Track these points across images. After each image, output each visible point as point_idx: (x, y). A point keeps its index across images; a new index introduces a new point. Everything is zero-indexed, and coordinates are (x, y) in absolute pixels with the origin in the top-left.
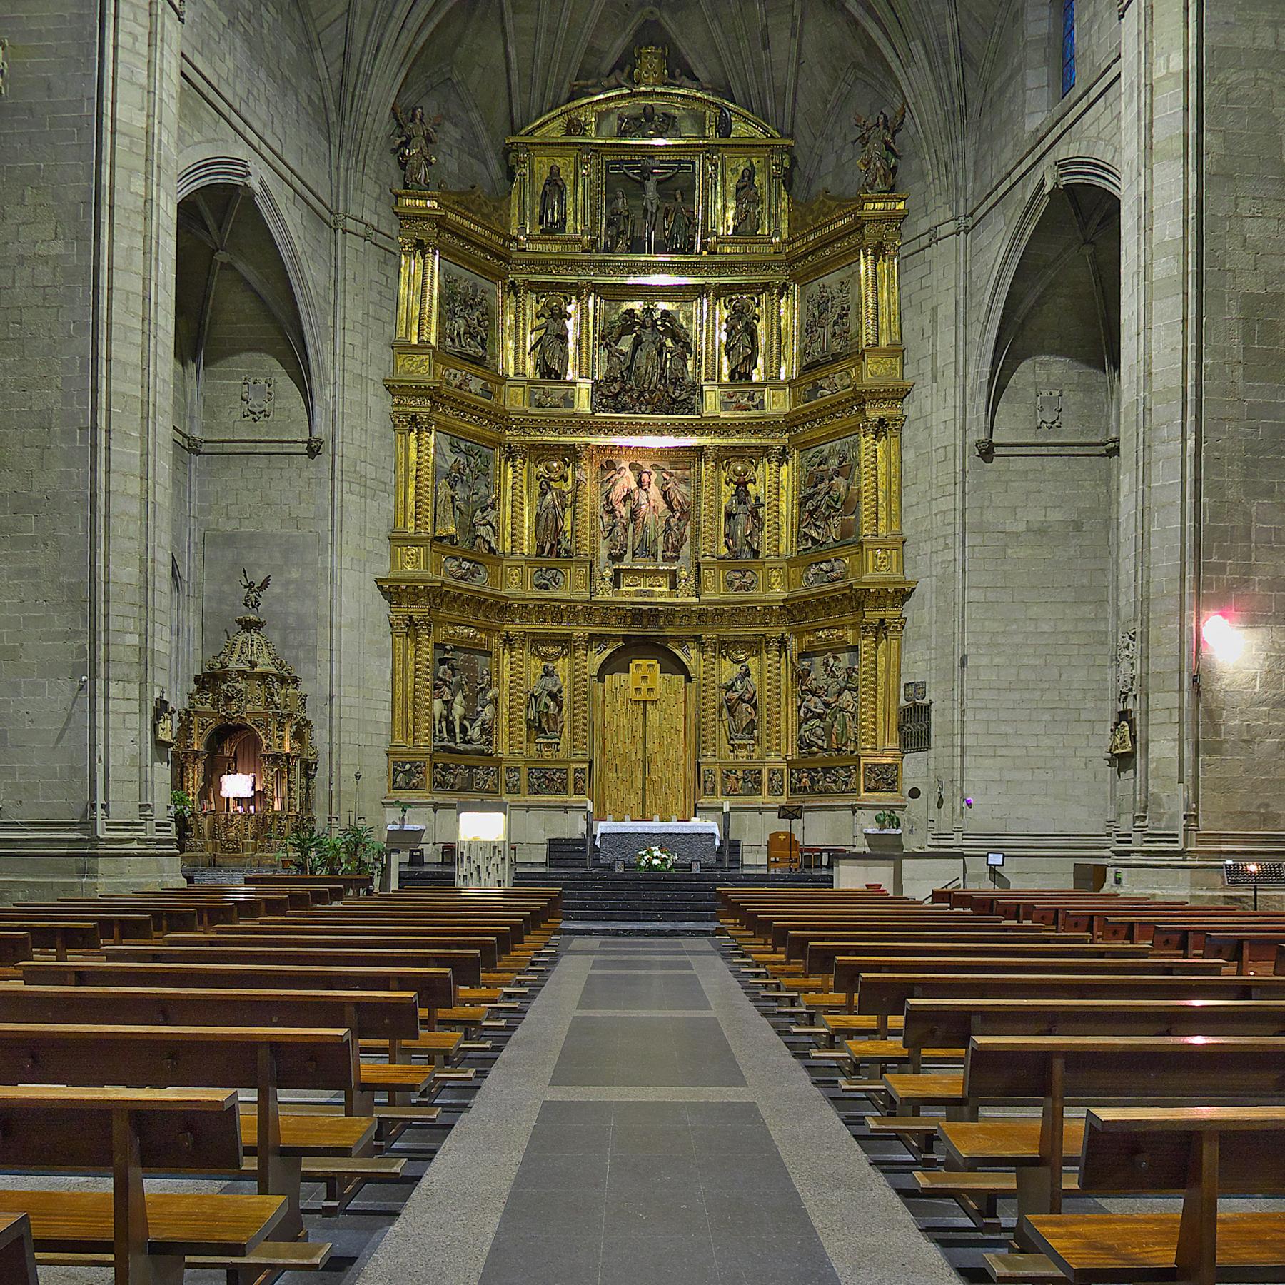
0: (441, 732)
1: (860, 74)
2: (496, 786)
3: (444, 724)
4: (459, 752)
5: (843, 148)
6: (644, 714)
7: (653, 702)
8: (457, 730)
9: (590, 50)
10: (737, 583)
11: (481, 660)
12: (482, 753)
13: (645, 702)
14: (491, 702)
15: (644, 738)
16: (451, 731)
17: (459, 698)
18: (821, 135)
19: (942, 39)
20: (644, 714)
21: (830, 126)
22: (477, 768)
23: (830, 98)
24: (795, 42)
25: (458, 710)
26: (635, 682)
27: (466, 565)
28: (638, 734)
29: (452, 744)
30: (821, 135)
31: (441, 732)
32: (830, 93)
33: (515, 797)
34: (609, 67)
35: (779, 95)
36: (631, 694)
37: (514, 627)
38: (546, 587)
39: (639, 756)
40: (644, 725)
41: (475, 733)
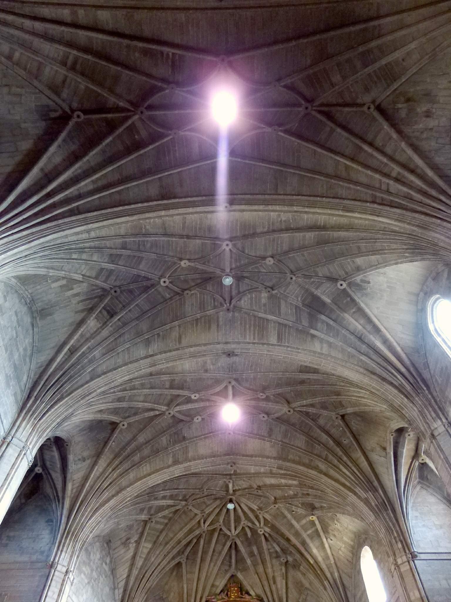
1: (309, 592)
9: (213, 586)
19: (335, 580)
24: (284, 581)
32: (299, 598)
34: (219, 591)
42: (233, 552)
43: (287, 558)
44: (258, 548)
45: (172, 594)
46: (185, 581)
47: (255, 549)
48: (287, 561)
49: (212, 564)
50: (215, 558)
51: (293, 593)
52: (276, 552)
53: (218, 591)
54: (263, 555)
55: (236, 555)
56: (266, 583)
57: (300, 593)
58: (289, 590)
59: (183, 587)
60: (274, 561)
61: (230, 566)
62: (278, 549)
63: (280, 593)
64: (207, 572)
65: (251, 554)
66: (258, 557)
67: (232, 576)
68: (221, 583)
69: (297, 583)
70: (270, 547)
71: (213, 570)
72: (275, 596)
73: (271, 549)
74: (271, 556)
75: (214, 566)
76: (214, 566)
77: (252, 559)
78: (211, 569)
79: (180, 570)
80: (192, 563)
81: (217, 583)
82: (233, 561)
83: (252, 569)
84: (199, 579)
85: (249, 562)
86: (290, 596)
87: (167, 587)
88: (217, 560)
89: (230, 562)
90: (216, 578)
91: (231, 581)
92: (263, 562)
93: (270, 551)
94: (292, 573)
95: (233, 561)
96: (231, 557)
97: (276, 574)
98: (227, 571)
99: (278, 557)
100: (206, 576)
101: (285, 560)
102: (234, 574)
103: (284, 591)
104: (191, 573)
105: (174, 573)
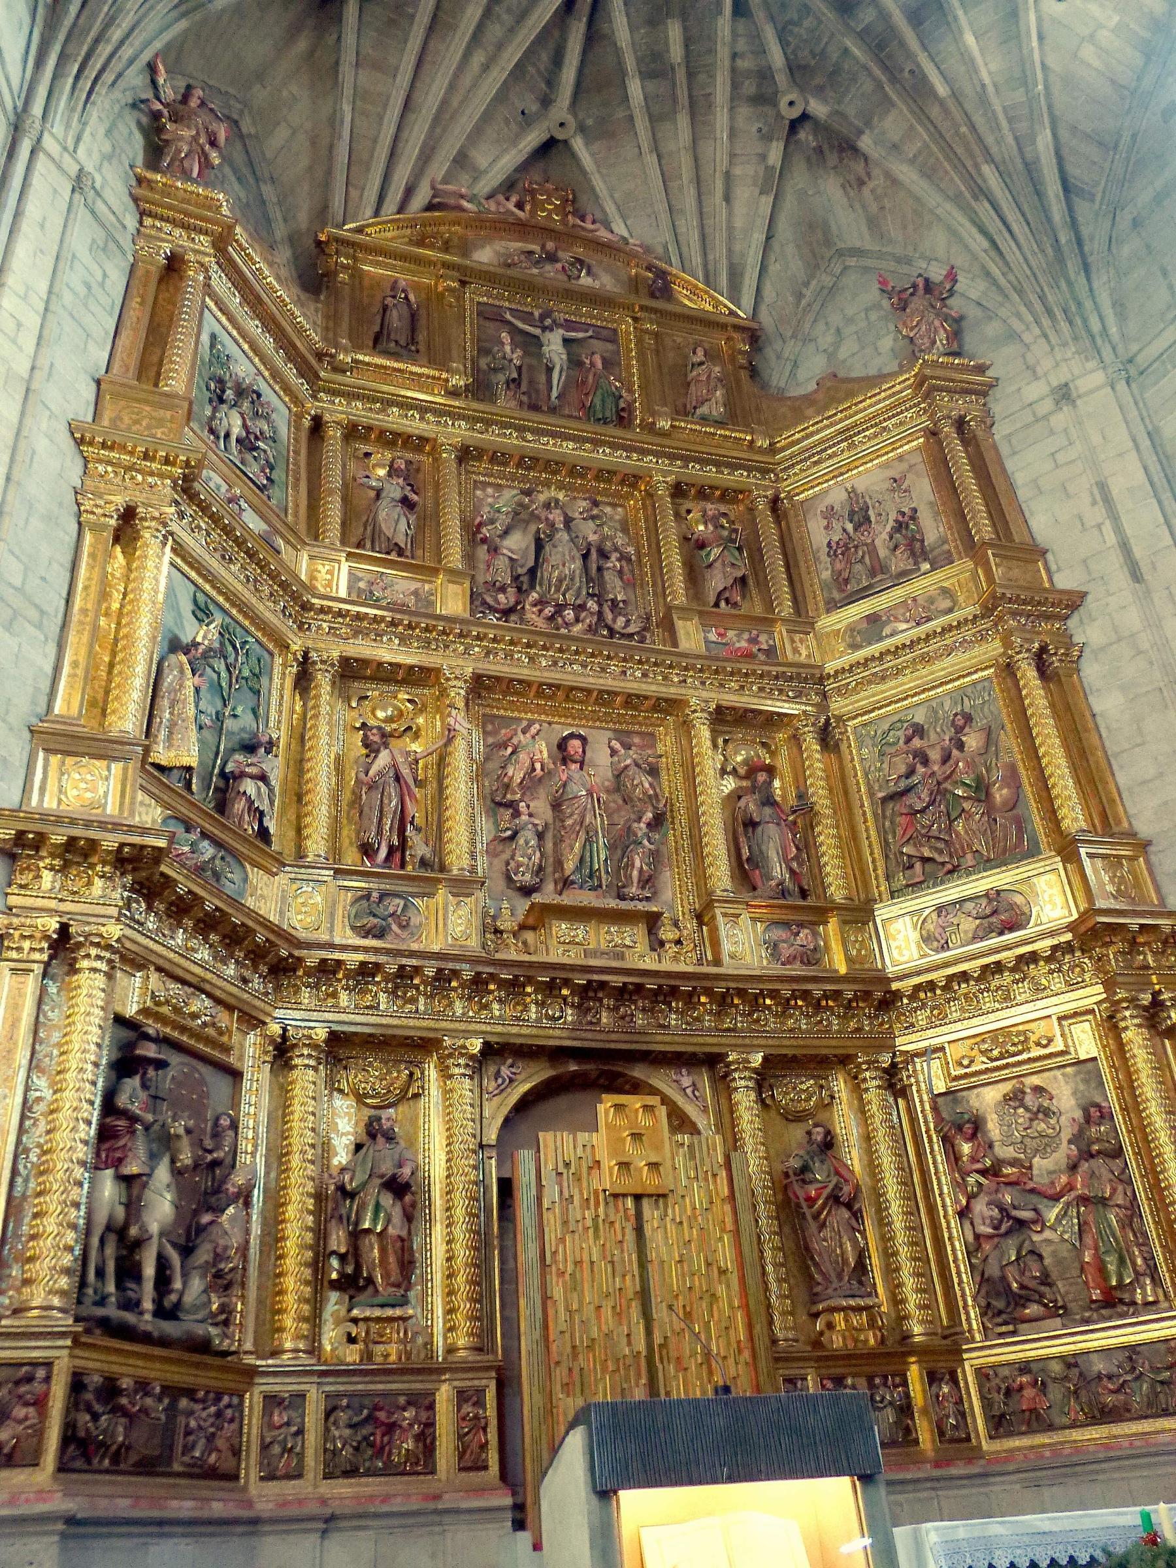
0: (100, 1273)
2: (236, 1452)
3: (110, 1251)
4: (146, 1338)
5: (837, 345)
6: (639, 1230)
7: (660, 1197)
8: (149, 1271)
9: (461, 160)
10: (786, 951)
11: (219, 1085)
12: (203, 1346)
13: (638, 1198)
14: (237, 1196)
15: (644, 1295)
16: (128, 1271)
17: (162, 1174)
18: (794, 336)
20: (639, 1230)
21: (807, 326)
22: (190, 1393)
23: (804, 291)
24: (767, 202)
25: (161, 1208)
26: (616, 1145)
27: (207, 850)
28: (632, 1285)
29: (130, 1317)
30: (794, 336)
31: (100, 1273)
32: (806, 284)
33: (290, 1488)
35: (735, 276)
36: (608, 1178)
37: (307, 1016)
38: (380, 934)
39: (641, 1345)
40: (643, 1263)
41: (192, 1288)
42: (577, 30)
43: (807, 103)
44: (688, 42)
45: (282, 134)
46: (348, 91)
47: (674, 32)
48: (805, 117)
49: (478, 58)
50: (495, 31)
51: (789, 261)
52: (764, 75)
53: (484, 186)
54: (702, 77)
55: (585, 52)
56: (688, 199)
57: (814, 265)
58: (776, 244)
59: (333, 121)
60: (744, 111)
61: (546, 102)
62: (777, 57)
63: (737, 247)
64: (452, 87)
65: (655, 67)
66: (681, 75)
67: (549, 147)
68: (499, 161)
69: (811, 227)
70: (742, 45)
71: (475, 85)
72: (719, 252)
73: (742, 56)
74: (735, 85)
75: (486, 68)
76: (486, 68)
77: (651, 86)
78: (467, 80)
79: (331, 40)
80: (392, 22)
81: (481, 158)
82: (569, 74)
83: (641, 124)
84: (408, 105)
85: (635, 88)
86: (774, 268)
87: (260, 95)
88: (500, 46)
89: (551, 82)
90: (478, 131)
91: (536, 175)
92: (699, 108)
93: (739, 62)
94: (799, 178)
95: (569, 74)
96: (558, 60)
97: (737, 171)
98: (527, 119)
99: (764, 99)
100: (445, 103)
101: (795, 113)
102: (560, 136)
103: (759, 237)
104: (377, 66)
105: (302, 44)
